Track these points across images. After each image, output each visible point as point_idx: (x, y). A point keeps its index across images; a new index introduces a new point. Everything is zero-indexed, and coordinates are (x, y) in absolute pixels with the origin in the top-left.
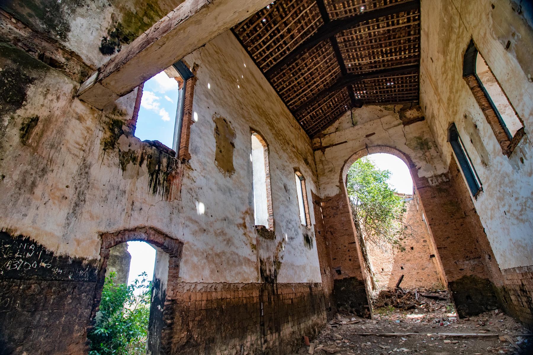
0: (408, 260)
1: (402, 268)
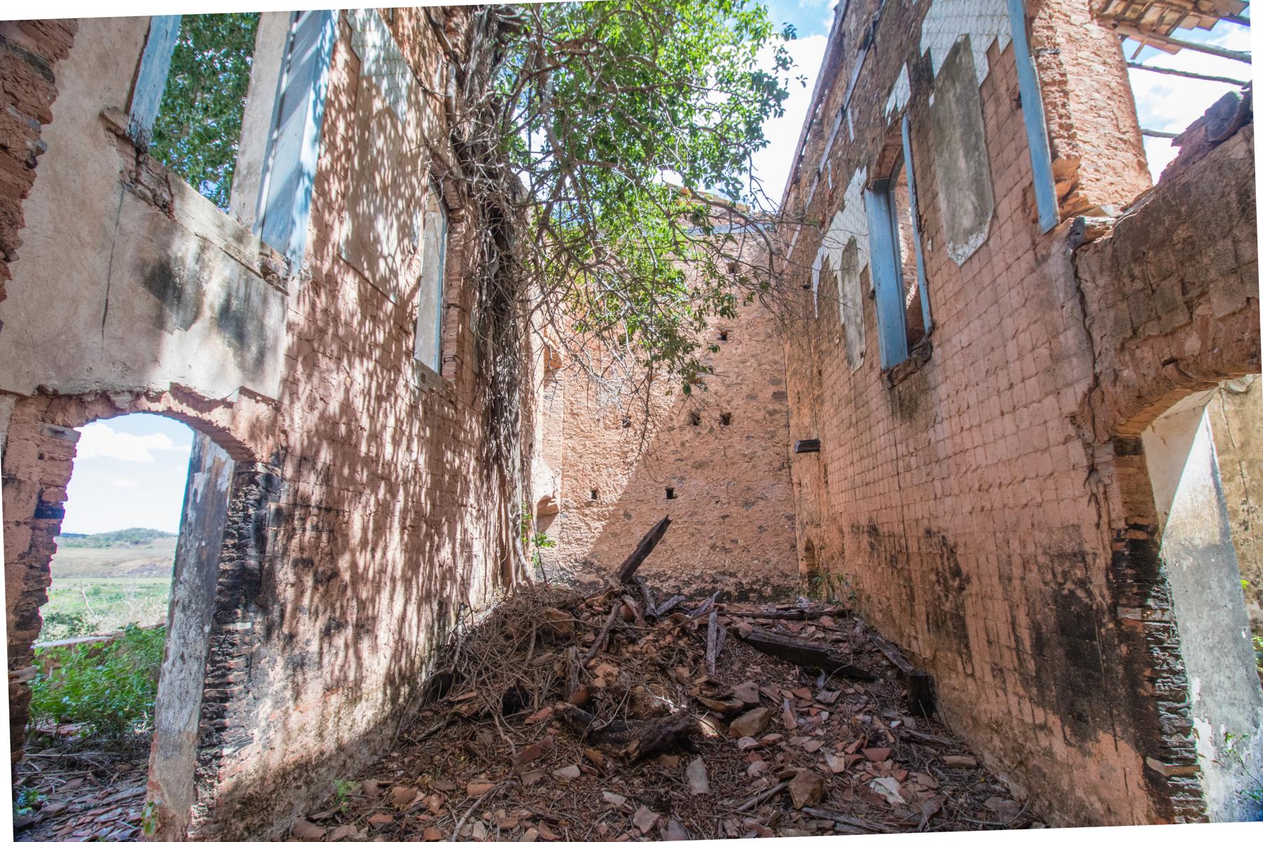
0: (700, 466)
1: (670, 494)
